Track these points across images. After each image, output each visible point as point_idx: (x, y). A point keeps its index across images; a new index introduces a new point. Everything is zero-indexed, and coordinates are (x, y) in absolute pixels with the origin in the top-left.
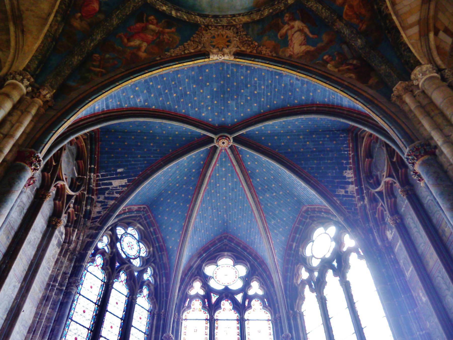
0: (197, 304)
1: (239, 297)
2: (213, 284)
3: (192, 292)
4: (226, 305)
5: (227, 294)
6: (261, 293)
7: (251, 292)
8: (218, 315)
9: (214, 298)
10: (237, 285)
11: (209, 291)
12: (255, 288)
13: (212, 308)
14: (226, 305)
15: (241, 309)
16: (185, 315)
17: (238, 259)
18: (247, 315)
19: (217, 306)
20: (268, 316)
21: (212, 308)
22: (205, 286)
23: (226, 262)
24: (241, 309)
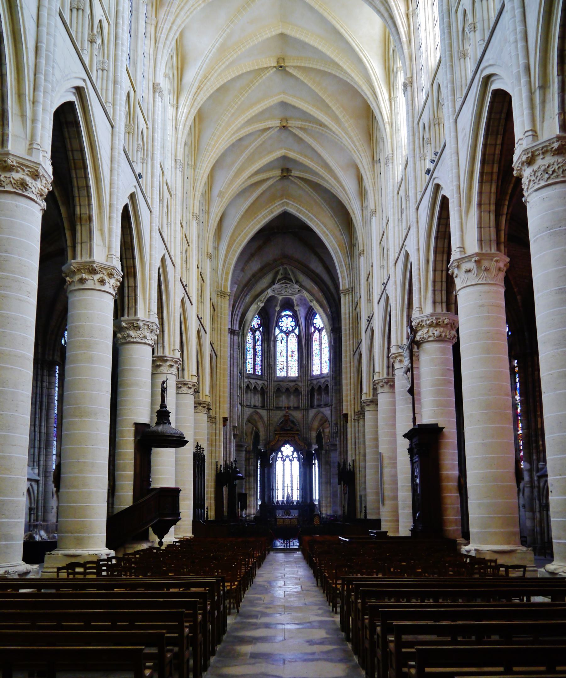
0: (280, 459)
1: (291, 458)
2: (284, 454)
3: (278, 456)
4: (287, 459)
5: (288, 456)
6: (297, 456)
7: (294, 456)
8: (285, 462)
9: (284, 458)
10: (290, 454)
11: (283, 456)
12: (295, 455)
13: (284, 461)
14: (287, 459)
15: (291, 461)
16: (277, 462)
17: (291, 445)
18: (293, 462)
19: (285, 460)
20: (298, 463)
21: (284, 461)
22: (282, 454)
23: (287, 446)
24: (291, 461)
